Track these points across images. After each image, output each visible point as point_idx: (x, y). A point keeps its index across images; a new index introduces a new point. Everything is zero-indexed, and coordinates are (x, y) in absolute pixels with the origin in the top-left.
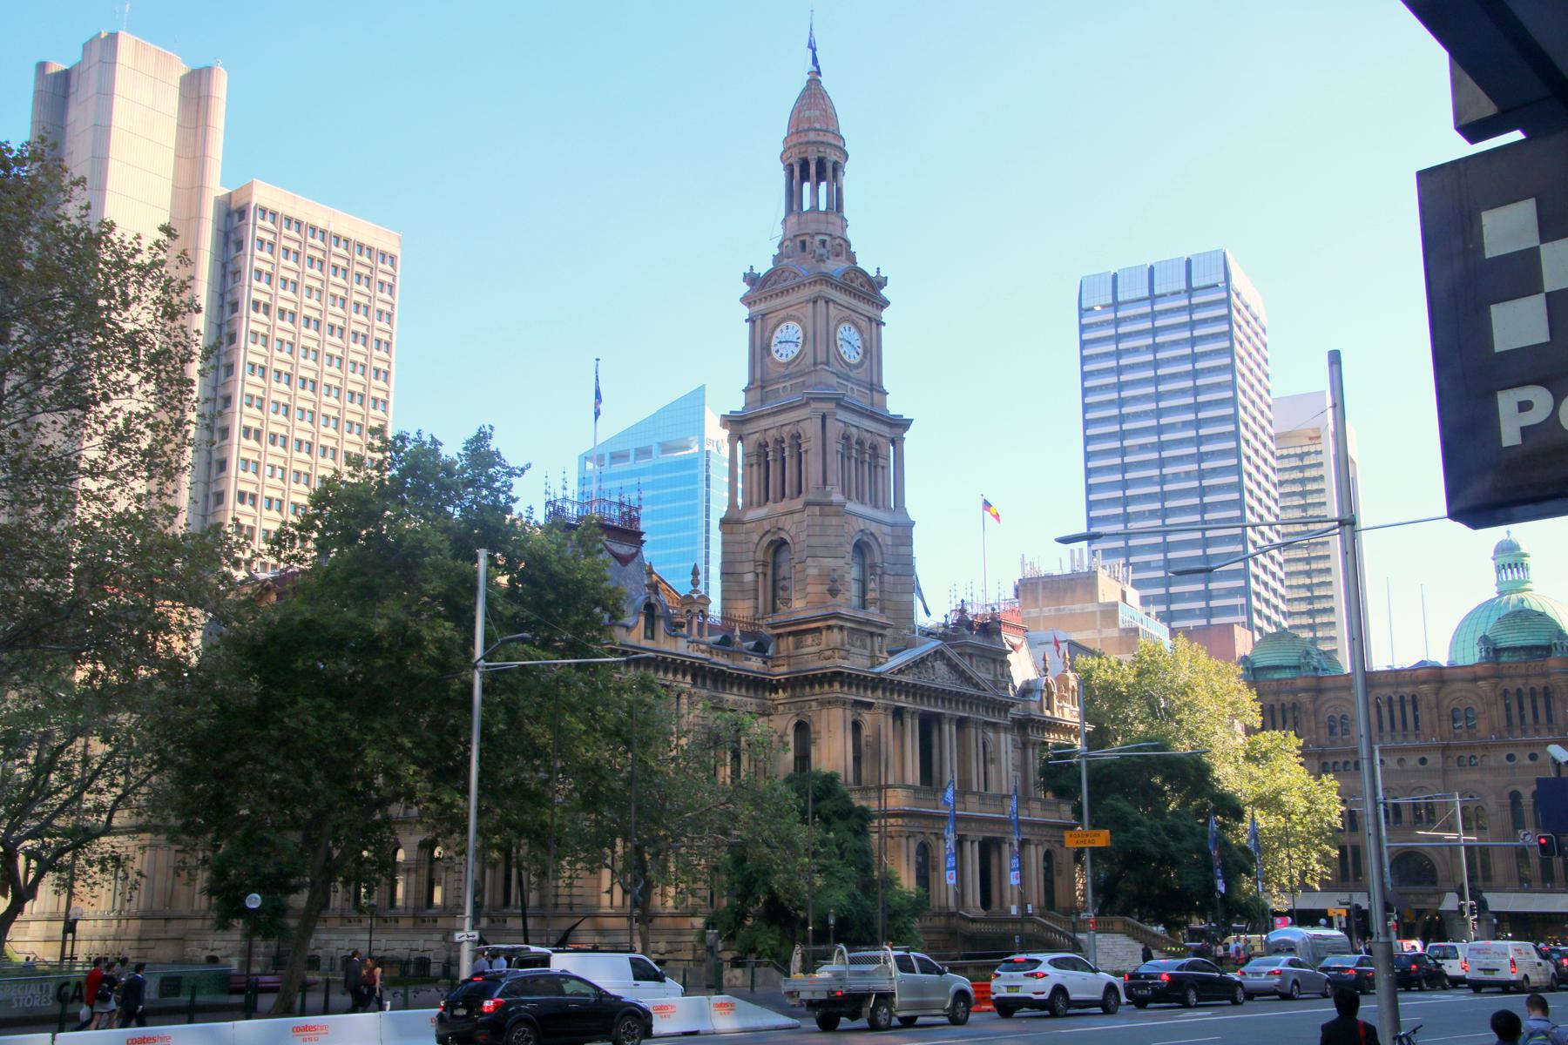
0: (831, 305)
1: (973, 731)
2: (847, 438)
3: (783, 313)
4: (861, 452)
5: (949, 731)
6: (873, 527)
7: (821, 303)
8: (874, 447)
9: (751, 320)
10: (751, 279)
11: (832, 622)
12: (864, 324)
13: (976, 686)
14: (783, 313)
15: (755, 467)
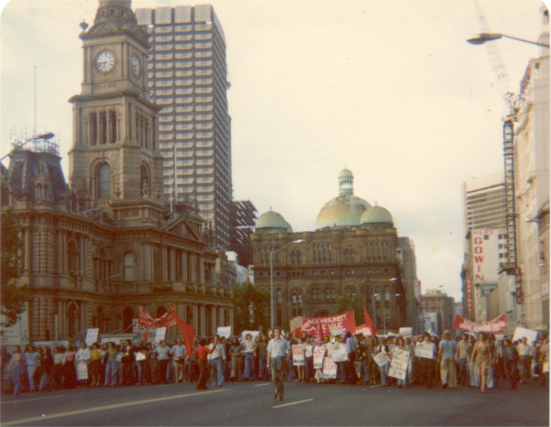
0: (130, 47)
1: (192, 256)
2: (137, 114)
3: (102, 47)
4: (142, 121)
5: (184, 256)
6: (147, 159)
7: (125, 46)
8: (146, 120)
9: (85, 48)
10: (84, 25)
11: (144, 206)
12: (141, 58)
13: (195, 236)
14: (102, 47)
15: (89, 125)
